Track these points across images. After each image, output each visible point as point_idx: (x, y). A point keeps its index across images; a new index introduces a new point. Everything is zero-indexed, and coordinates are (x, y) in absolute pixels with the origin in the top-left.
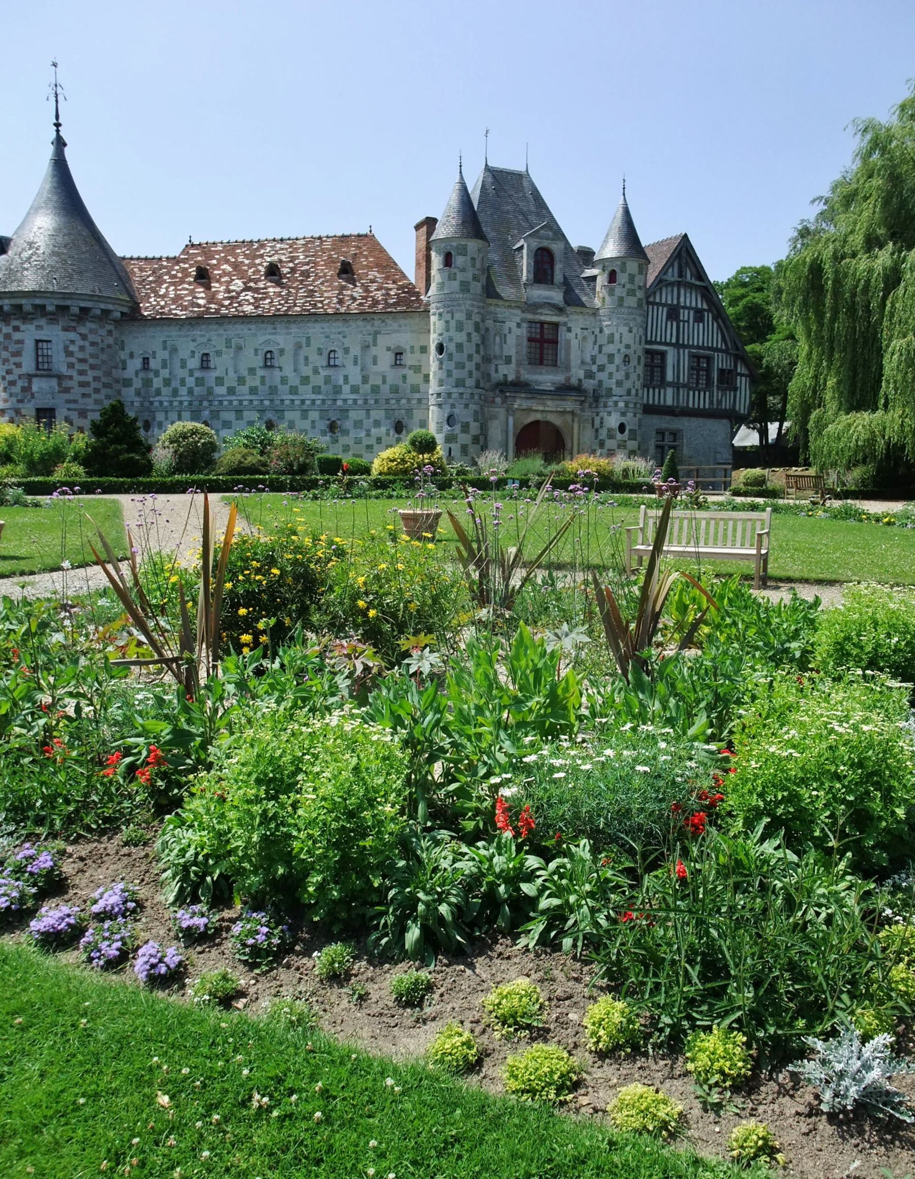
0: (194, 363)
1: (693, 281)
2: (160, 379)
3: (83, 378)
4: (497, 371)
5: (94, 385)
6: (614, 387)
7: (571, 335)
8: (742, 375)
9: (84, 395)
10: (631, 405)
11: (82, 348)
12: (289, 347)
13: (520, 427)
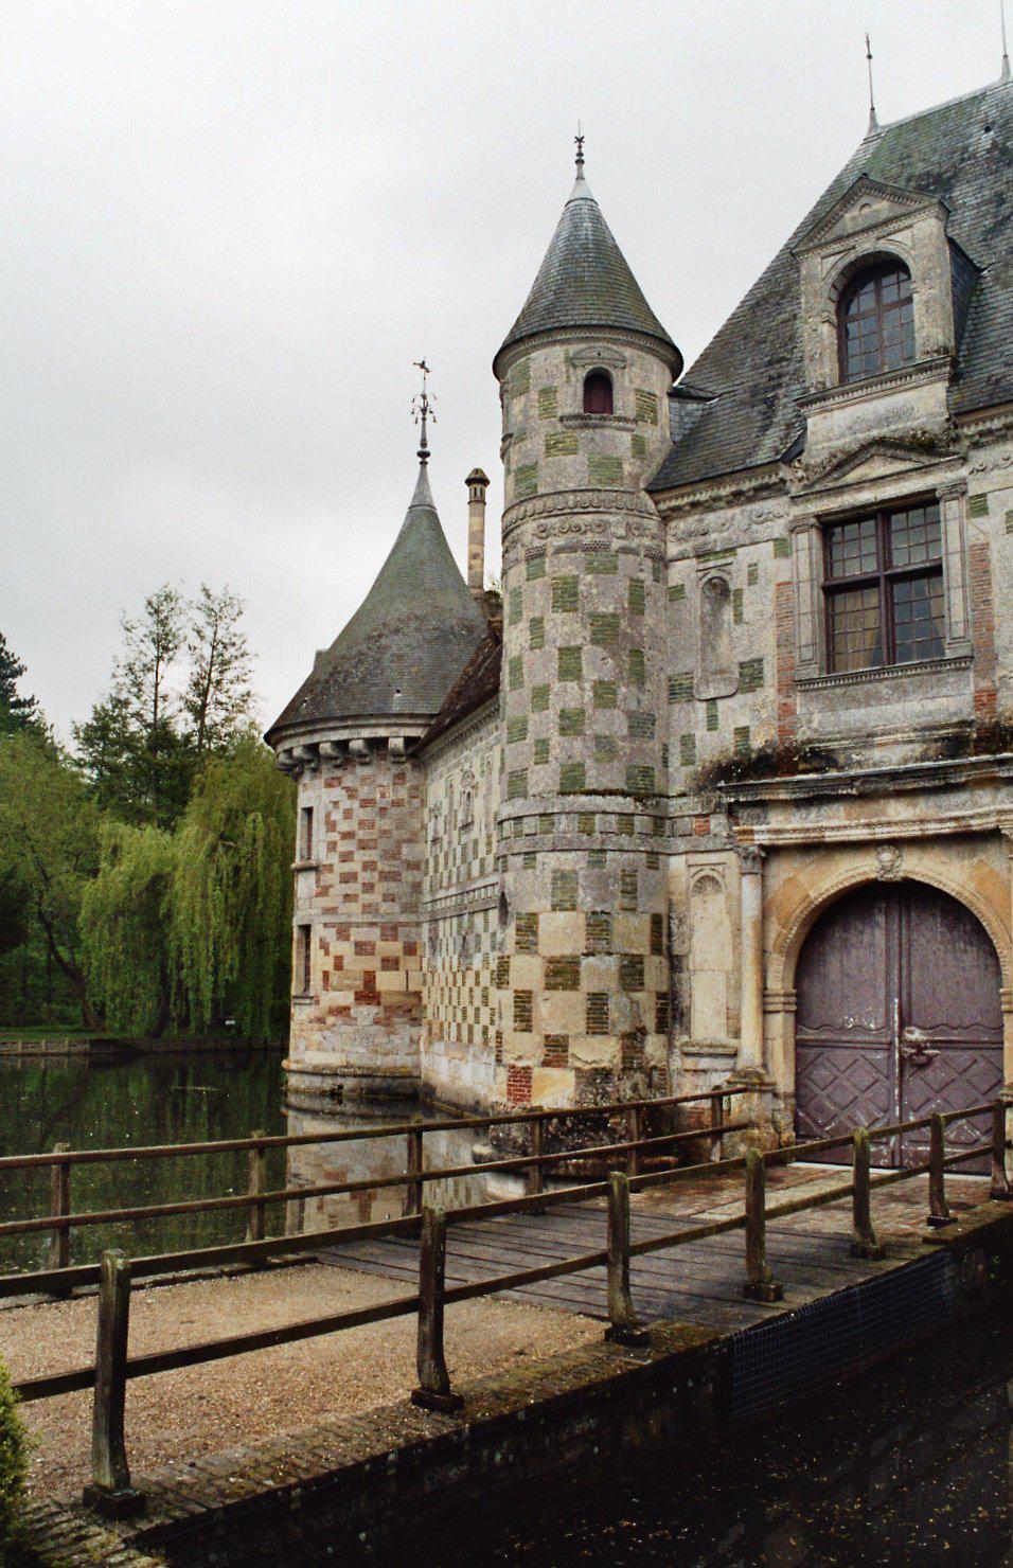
3: (347, 867)
5: (364, 877)
9: (347, 898)
11: (348, 814)
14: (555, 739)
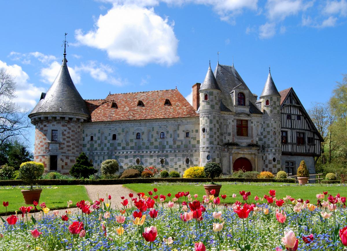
0: (111, 137)
1: (296, 105)
2: (97, 144)
3: (68, 144)
4: (225, 139)
5: (72, 146)
6: (270, 144)
7: (253, 125)
8: (316, 139)
9: (68, 150)
10: (278, 151)
11: (69, 133)
12: (146, 132)
13: (235, 160)
14: (217, 139)
